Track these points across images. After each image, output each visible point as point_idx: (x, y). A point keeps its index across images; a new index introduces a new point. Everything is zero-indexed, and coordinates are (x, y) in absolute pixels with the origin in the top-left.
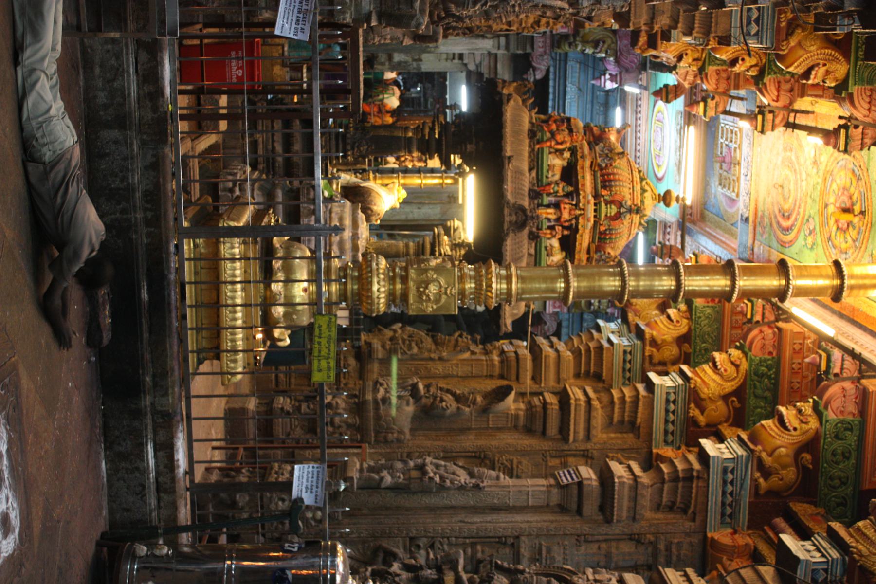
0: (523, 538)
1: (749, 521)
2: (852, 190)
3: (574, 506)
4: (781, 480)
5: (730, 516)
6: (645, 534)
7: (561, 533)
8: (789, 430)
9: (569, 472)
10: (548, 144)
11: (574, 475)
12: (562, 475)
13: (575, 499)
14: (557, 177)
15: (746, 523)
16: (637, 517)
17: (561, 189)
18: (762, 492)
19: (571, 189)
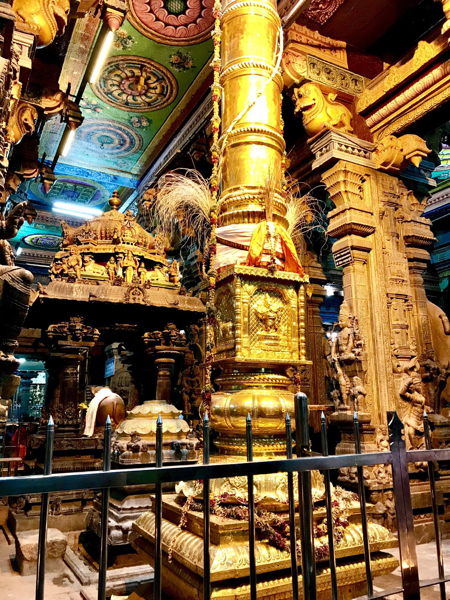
0: (388, 291)
1: (369, 141)
2: (123, 75)
3: (366, 253)
4: (345, 115)
5: (366, 153)
6: (380, 209)
7: (382, 264)
8: (315, 104)
9: (336, 259)
10: (78, 271)
11: (342, 254)
12: (340, 263)
13: (361, 252)
14: (103, 268)
15: (370, 143)
16: (371, 212)
17: (111, 264)
18: (352, 129)
19: (112, 258)
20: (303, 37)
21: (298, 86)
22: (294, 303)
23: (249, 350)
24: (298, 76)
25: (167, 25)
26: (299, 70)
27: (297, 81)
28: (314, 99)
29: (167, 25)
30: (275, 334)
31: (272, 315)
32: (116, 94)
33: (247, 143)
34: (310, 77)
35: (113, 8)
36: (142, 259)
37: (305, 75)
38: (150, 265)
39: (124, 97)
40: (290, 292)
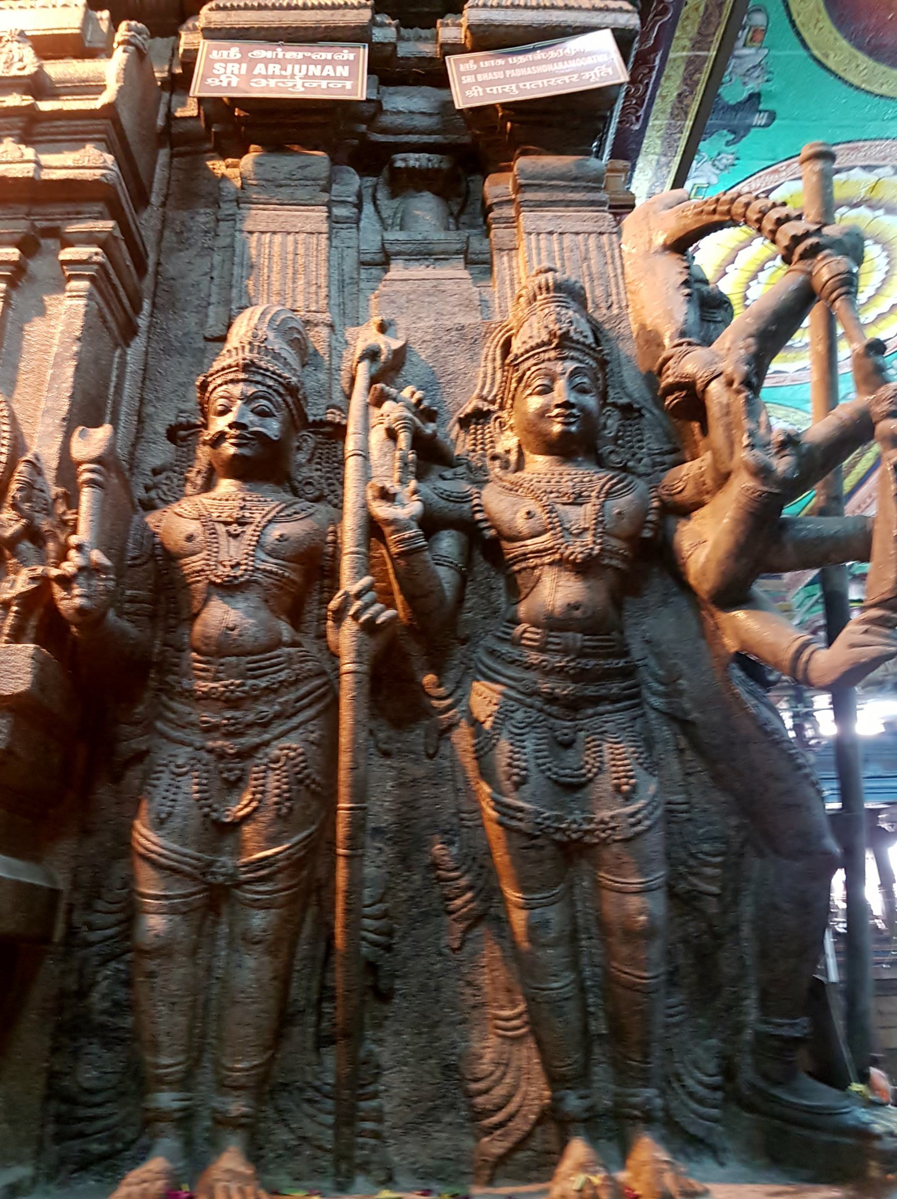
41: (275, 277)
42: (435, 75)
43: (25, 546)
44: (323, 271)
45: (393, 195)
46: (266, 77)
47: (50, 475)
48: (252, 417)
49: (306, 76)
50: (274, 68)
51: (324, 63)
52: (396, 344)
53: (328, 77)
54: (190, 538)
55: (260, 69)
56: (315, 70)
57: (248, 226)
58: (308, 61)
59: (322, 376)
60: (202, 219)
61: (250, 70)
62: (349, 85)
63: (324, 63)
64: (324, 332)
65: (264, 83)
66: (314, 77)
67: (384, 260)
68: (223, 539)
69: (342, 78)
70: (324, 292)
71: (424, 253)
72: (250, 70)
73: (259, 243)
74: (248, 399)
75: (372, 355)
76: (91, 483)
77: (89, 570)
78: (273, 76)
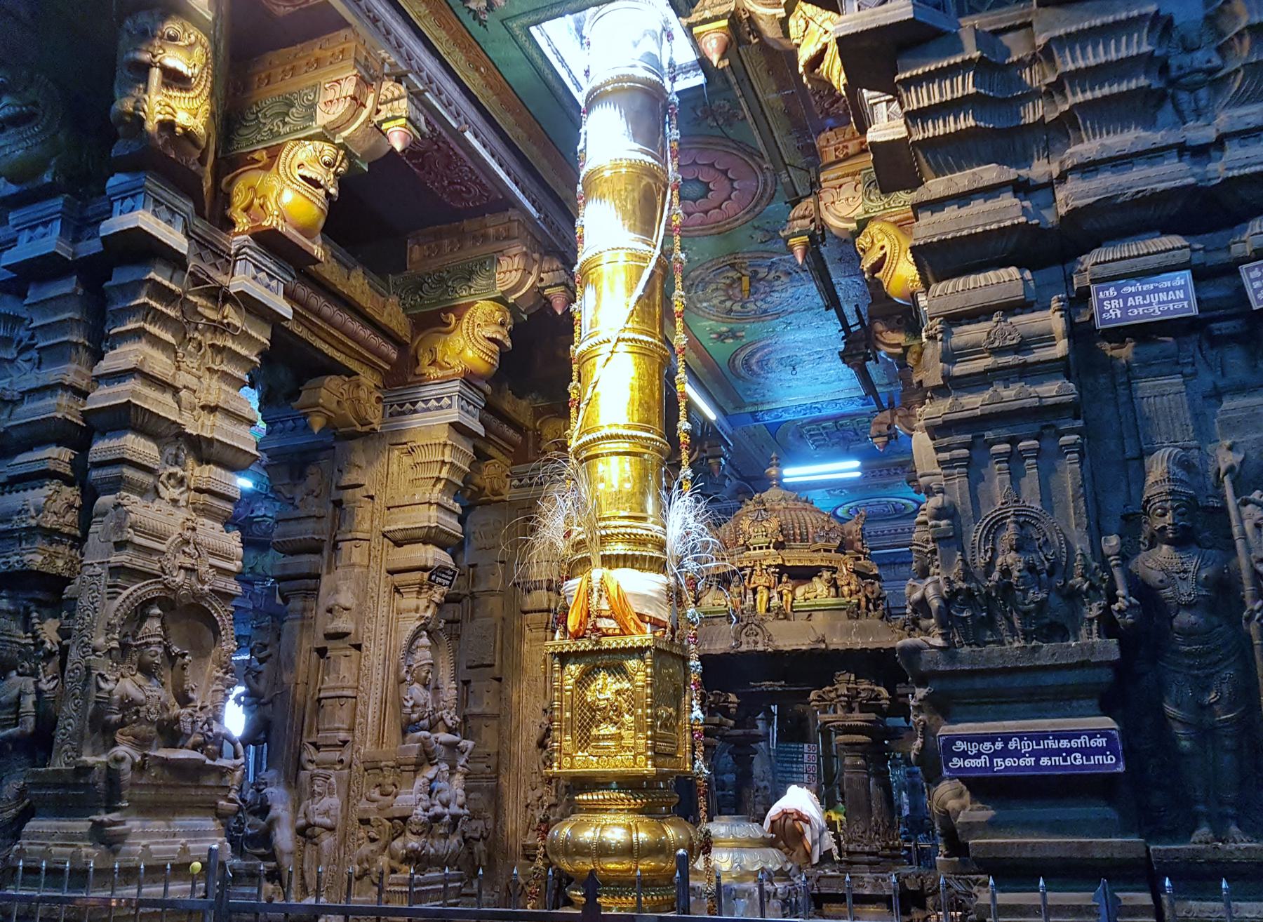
20: (850, 144)
21: (857, 233)
22: (640, 678)
23: (572, 758)
24: (851, 220)
25: (706, 212)
26: (845, 211)
27: (853, 226)
28: (882, 248)
29: (706, 212)
30: (612, 730)
31: (603, 704)
32: (737, 307)
33: (597, 456)
34: (867, 212)
35: (550, 287)
36: (782, 569)
37: (859, 212)
38: (803, 575)
39: (751, 306)
40: (632, 664)
41: (1162, 424)
42: (1231, 269)
43: (1091, 592)
44: (1188, 415)
45: (1212, 347)
46: (1136, 307)
47: (1089, 557)
48: (1178, 518)
49: (1159, 303)
50: (1139, 299)
51: (1167, 290)
52: (1240, 457)
53: (1172, 301)
54: (1161, 581)
55: (1131, 301)
56: (1163, 297)
57: (1139, 394)
58: (1157, 290)
59: (1201, 479)
60: (1102, 381)
61: (1125, 302)
62: (1185, 303)
63: (1167, 290)
64: (1196, 452)
65: (1136, 312)
66: (1164, 302)
67: (1217, 395)
68: (1179, 582)
69: (1180, 300)
70: (1191, 428)
71: (1241, 389)
72: (1125, 302)
73: (1149, 405)
74: (1174, 509)
75: (1230, 470)
76: (1117, 565)
77: (1131, 606)
78: (1140, 306)
